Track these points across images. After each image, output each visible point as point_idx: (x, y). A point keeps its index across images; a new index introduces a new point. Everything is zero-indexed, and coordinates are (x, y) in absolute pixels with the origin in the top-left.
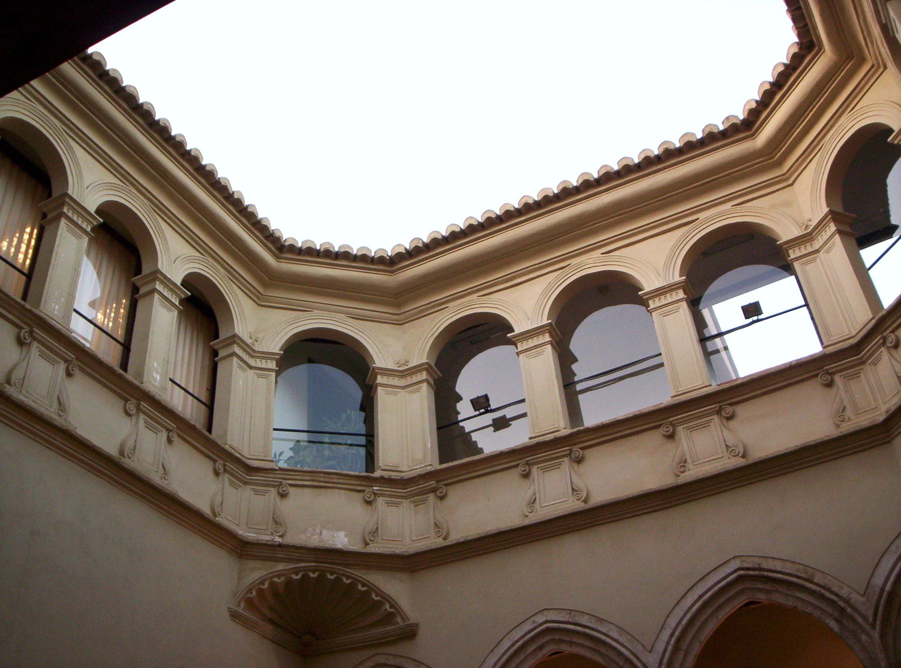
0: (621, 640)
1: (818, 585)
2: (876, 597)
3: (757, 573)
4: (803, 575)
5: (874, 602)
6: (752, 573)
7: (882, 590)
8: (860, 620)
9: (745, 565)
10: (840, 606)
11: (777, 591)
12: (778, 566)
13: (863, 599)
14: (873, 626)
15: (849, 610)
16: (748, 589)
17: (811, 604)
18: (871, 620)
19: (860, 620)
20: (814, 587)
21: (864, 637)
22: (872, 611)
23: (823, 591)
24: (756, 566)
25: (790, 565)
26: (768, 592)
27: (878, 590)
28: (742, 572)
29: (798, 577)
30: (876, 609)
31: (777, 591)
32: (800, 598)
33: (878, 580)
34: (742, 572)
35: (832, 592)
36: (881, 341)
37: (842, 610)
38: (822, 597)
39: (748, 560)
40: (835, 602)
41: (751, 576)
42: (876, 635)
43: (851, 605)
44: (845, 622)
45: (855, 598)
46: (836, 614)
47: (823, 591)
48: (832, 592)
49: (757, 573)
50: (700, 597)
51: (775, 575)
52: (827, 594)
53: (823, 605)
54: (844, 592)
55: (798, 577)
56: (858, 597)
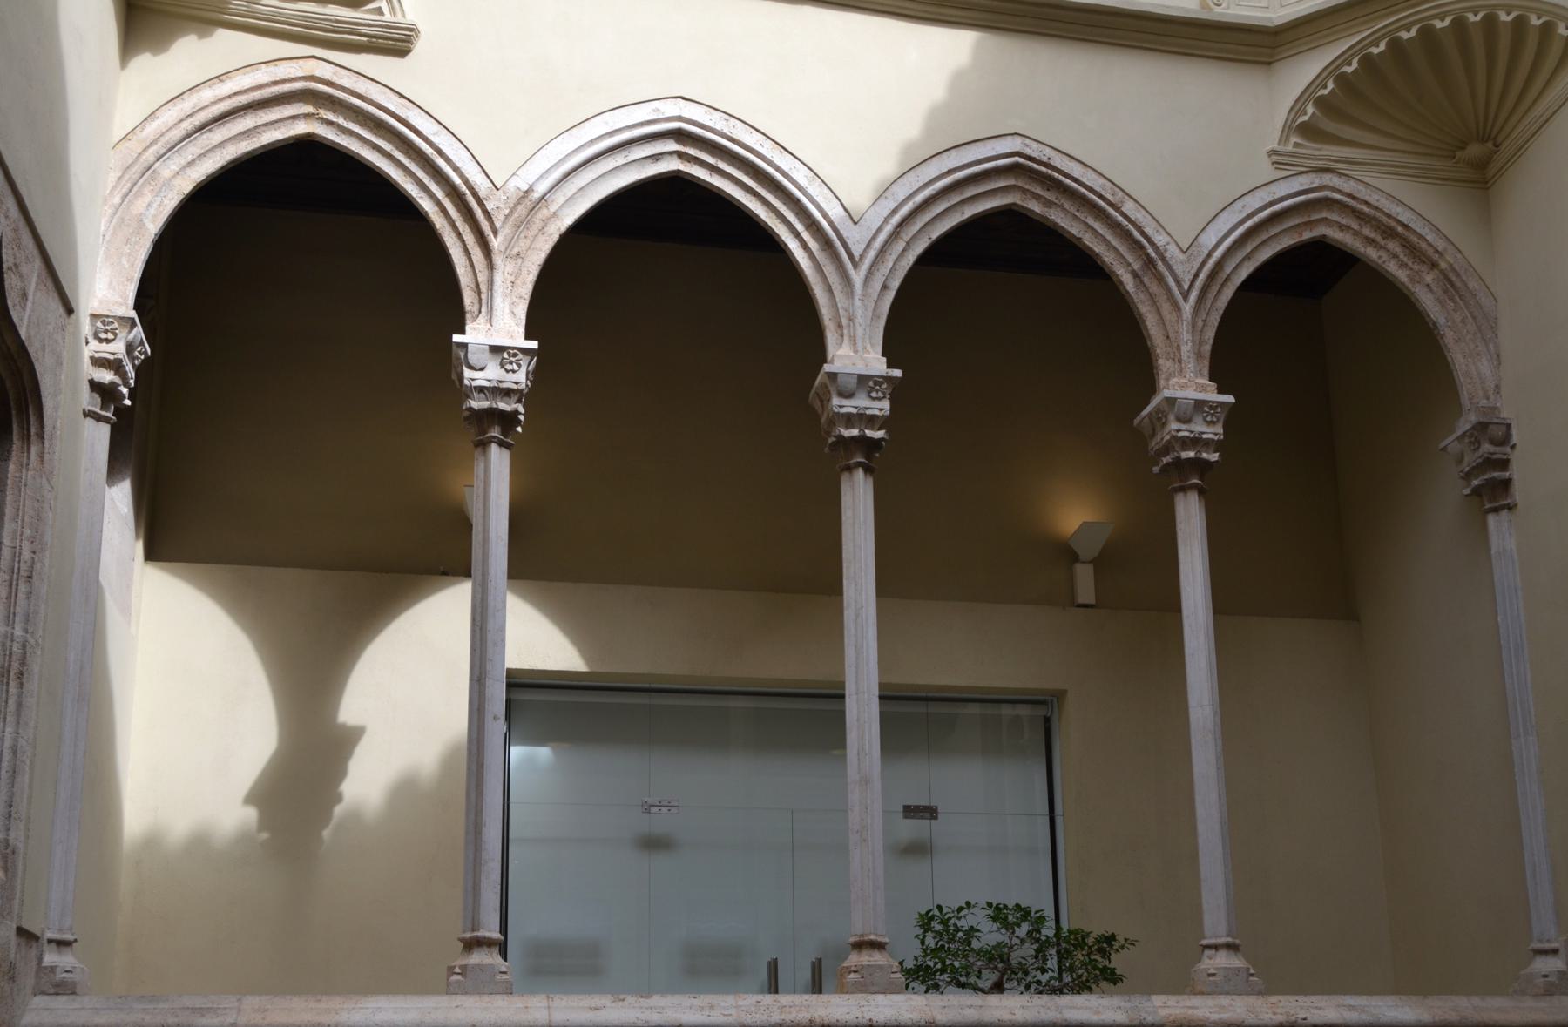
0: (810, 190)
3: (1043, 169)
4: (1110, 198)
5: (1196, 266)
6: (1036, 166)
7: (1209, 255)
8: (1172, 283)
9: (1028, 151)
10: (1148, 255)
11: (1062, 206)
12: (1076, 170)
13: (1182, 257)
14: (1186, 296)
15: (1160, 263)
16: (1020, 188)
17: (1105, 240)
19: (1172, 283)
20: (1120, 218)
21: (1166, 307)
24: (1045, 159)
26: (1048, 204)
28: (1021, 160)
29: (1101, 197)
30: (1196, 275)
31: (1062, 206)
33: (1209, 239)
34: (1021, 160)
35: (1143, 234)
37: (1149, 262)
38: (1126, 236)
39: (1035, 145)
40: (1142, 247)
41: (1031, 170)
42: (1187, 308)
43: (1163, 259)
44: (1146, 280)
45: (1172, 252)
46: (1136, 266)
49: (1043, 169)
50: (950, 172)
51: (1068, 181)
52: (1136, 234)
53: (1122, 249)
54: (1160, 239)
55: (1101, 197)
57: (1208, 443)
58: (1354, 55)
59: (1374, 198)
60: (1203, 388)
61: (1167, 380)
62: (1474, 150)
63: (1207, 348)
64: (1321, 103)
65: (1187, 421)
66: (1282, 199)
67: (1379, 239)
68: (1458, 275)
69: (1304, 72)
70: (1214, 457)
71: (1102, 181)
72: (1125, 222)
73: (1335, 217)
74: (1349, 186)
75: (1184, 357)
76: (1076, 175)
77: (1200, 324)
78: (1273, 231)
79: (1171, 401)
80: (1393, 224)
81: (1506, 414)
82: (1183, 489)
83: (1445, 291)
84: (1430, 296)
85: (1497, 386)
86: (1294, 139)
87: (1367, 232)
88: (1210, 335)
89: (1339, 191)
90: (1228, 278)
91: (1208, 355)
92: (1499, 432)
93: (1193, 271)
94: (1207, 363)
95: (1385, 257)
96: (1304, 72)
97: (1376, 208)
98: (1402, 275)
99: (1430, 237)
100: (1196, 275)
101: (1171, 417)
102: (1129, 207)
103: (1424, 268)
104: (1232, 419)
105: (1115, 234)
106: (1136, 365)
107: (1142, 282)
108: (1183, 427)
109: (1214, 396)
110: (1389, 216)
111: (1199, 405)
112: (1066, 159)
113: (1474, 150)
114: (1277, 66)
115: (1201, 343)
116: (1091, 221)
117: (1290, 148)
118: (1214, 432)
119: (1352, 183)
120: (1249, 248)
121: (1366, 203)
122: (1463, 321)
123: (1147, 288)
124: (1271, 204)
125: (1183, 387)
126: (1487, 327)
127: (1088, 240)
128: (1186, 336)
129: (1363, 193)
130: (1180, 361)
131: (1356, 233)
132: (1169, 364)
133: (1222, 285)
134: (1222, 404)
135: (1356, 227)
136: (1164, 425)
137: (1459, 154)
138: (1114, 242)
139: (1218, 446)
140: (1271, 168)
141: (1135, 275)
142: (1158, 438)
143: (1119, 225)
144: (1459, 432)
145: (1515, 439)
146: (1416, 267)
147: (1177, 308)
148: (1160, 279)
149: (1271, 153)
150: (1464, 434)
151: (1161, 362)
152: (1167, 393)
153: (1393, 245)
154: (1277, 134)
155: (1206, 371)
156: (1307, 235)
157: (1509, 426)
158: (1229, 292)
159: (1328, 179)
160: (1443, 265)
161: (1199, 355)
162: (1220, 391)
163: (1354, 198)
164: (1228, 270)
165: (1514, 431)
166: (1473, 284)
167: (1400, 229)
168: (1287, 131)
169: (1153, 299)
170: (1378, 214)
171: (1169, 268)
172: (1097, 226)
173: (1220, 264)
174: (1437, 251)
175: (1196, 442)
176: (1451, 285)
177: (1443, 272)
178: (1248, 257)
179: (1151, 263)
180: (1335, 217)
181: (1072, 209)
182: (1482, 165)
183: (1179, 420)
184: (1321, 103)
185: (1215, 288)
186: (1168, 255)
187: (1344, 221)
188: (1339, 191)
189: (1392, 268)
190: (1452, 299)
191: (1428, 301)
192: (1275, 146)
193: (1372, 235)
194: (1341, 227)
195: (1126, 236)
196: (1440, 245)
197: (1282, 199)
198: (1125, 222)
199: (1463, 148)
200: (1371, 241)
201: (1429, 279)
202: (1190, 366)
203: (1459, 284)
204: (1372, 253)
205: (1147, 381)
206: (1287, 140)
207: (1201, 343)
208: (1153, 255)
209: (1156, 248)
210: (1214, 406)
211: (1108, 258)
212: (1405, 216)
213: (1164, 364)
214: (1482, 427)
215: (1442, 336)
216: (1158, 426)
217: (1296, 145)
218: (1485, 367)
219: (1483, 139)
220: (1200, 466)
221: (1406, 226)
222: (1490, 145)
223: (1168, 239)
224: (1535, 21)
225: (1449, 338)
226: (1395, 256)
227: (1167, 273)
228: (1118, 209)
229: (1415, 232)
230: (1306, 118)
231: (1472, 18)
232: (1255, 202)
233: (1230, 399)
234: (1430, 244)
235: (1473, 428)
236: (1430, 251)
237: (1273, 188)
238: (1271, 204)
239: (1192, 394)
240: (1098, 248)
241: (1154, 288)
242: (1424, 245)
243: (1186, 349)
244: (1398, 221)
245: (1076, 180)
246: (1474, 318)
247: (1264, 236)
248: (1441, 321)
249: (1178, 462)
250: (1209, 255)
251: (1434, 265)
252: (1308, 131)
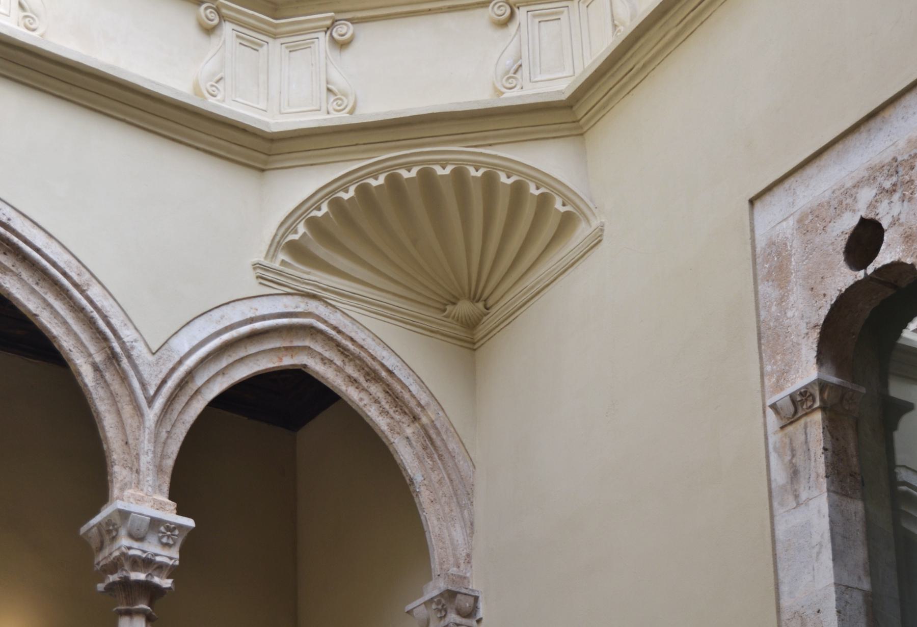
1: (91, 302)
2: (170, 365)
5: (165, 371)
7: (180, 362)
10: (112, 349)
12: (39, 239)
14: (151, 401)
15: (125, 363)
17: (65, 323)
18: (152, 392)
20: (84, 302)
21: (127, 411)
22: (159, 382)
23: (95, 315)
25: (58, 249)
27: (177, 359)
29: (65, 274)
30: (164, 382)
31: (18, 276)
32: (52, 307)
33: (182, 344)
35: (109, 324)
36: (329, 23)
37: (113, 357)
38: (90, 323)
40: (106, 339)
42: (151, 415)
43: (129, 357)
44: (108, 376)
45: (139, 351)
46: (98, 358)
47: (95, 315)
48: (109, 324)
53: (85, 337)
54: (127, 334)
55: (65, 274)
56: (145, 350)
57: (161, 567)
58: (351, 182)
59: (359, 336)
60: (161, 506)
61: (122, 489)
62: (464, 308)
63: (170, 463)
64: (313, 223)
65: (141, 539)
66: (264, 318)
67: (362, 380)
68: (439, 433)
69: (298, 187)
70: (167, 583)
71: (67, 257)
72: (89, 308)
73: (318, 348)
74: (336, 319)
75: (143, 467)
76: (39, 244)
77: (164, 435)
78: (252, 350)
79: (124, 515)
80: (378, 367)
81: (475, 585)
82: (129, 613)
83: (425, 448)
84: (408, 449)
85: (468, 555)
86: (282, 256)
87: (350, 370)
88: (174, 448)
89: (325, 322)
90: (198, 391)
91: (169, 470)
92: (467, 604)
93: (162, 376)
94: (167, 479)
95: (366, 400)
96: (298, 187)
97: (362, 347)
98: (381, 423)
99: (414, 388)
100: (164, 382)
101: (123, 532)
102: (95, 292)
103: (405, 419)
104: (191, 545)
105: (78, 319)
106: (90, 471)
107: (102, 377)
108: (135, 545)
109: (170, 515)
110: (374, 358)
111: (155, 523)
112: (28, 224)
113: (464, 308)
114: (269, 175)
115: (163, 456)
116: (51, 299)
117: (276, 265)
118: (169, 556)
119: (339, 315)
120: (224, 362)
121: (352, 340)
122: (440, 482)
123: (107, 385)
124: (252, 320)
125: (139, 500)
126: (462, 493)
127: (46, 319)
128: (146, 445)
129: (349, 328)
130: (138, 472)
131: (339, 370)
132: (125, 472)
133: (192, 398)
134: (180, 527)
135: (339, 362)
136: (114, 539)
137: (449, 308)
138: (76, 327)
139: (173, 572)
140: (255, 282)
141: (96, 368)
142: (106, 552)
143: (82, 309)
144: (427, 597)
145: (481, 613)
146: (397, 417)
147: (139, 412)
148: (124, 378)
149: (256, 266)
150: (431, 600)
151: (116, 468)
152: (120, 505)
153: (375, 389)
154: (264, 247)
155: (166, 488)
156: (288, 361)
157: (476, 599)
158: (198, 407)
159: (314, 306)
160: (424, 420)
161: (159, 469)
162: (180, 512)
163: (339, 332)
164: (200, 381)
165: (481, 605)
166: (452, 445)
167: (384, 374)
168: (276, 246)
169: (113, 396)
170: (363, 354)
171: (135, 367)
172: (58, 305)
173: (190, 375)
174: (419, 405)
175: (147, 563)
176: (430, 441)
177: (423, 427)
178: (222, 372)
179: (113, 358)
180: (318, 348)
181: (31, 281)
182: (471, 324)
183: (131, 536)
184: (313, 223)
185: (184, 399)
186: (134, 353)
187: (327, 354)
188: (325, 322)
189: (372, 413)
190: (430, 457)
191: (407, 455)
192: (260, 258)
193: (355, 375)
194: (324, 360)
195: (90, 323)
196: (424, 398)
197: (264, 318)
198: (89, 308)
199: (454, 304)
200: (354, 381)
201: (409, 431)
202: (149, 478)
203: (438, 443)
204: (352, 394)
205: (98, 488)
206: (274, 256)
207: (163, 456)
208: (118, 349)
209: (122, 344)
210: (172, 528)
211: (66, 343)
212: (391, 362)
213: (119, 473)
214: (451, 595)
215: (418, 494)
216: (107, 538)
217: (283, 263)
218: (458, 534)
219: (474, 298)
220: (151, 591)
221: (390, 372)
222: (480, 305)
223: (135, 335)
224: (533, 191)
225: (424, 497)
226: (377, 401)
227: (131, 373)
228: (82, 292)
229: (399, 381)
230: (296, 237)
231: (472, 172)
232: (235, 314)
233: (190, 522)
234: (413, 396)
235: (441, 595)
236: (413, 404)
237: (255, 303)
238: (252, 320)
239: (148, 510)
240: (55, 330)
241: (116, 386)
242: (407, 396)
243: (146, 460)
244: (383, 365)
245: (38, 250)
246: (451, 481)
247: (242, 353)
248: (418, 478)
249: (126, 585)
250: (180, 362)
251: (415, 418)
252: (297, 250)
